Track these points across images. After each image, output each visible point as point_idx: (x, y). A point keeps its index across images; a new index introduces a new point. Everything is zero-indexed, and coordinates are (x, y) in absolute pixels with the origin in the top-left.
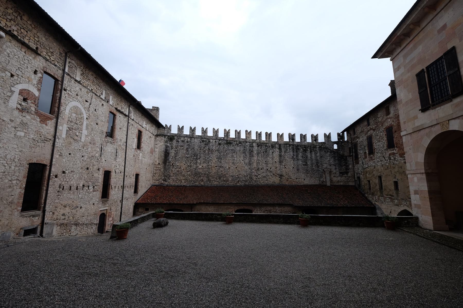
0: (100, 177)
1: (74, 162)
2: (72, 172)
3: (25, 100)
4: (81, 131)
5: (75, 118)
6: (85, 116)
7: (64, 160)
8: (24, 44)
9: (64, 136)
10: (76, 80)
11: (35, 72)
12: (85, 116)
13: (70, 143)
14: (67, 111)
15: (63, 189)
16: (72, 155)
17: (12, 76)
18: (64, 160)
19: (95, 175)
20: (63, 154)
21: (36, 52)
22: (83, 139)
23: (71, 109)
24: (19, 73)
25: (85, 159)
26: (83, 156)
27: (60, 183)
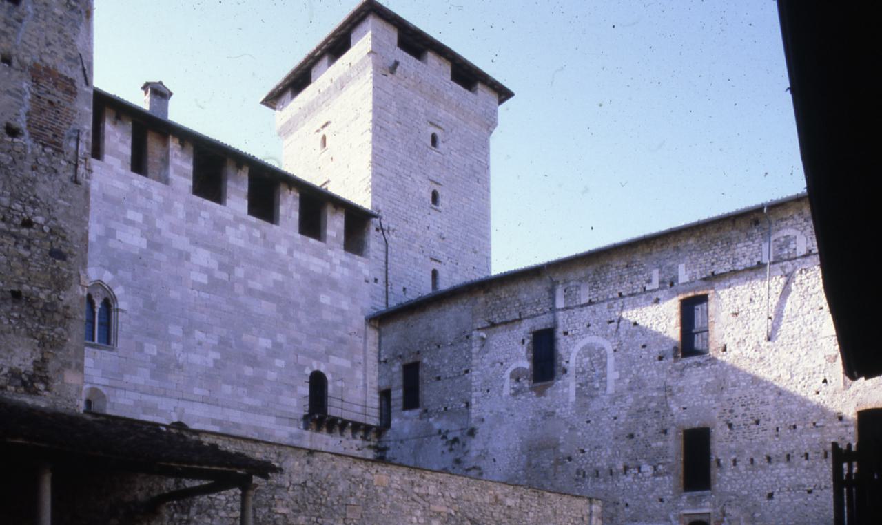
0: (673, 447)
1: (598, 431)
2: (596, 448)
3: (518, 380)
4: (604, 379)
5: (589, 363)
6: (609, 350)
7: (579, 434)
8: (506, 323)
9: (573, 398)
10: (582, 306)
11: (523, 342)
12: (609, 350)
13: (586, 405)
14: (572, 361)
15: (584, 476)
16: (593, 422)
17: (502, 364)
18: (579, 434)
19: (654, 445)
20: (576, 426)
21: (520, 320)
22: (611, 389)
23: (579, 354)
24: (508, 356)
25: (622, 421)
26: (615, 418)
27: (578, 467)
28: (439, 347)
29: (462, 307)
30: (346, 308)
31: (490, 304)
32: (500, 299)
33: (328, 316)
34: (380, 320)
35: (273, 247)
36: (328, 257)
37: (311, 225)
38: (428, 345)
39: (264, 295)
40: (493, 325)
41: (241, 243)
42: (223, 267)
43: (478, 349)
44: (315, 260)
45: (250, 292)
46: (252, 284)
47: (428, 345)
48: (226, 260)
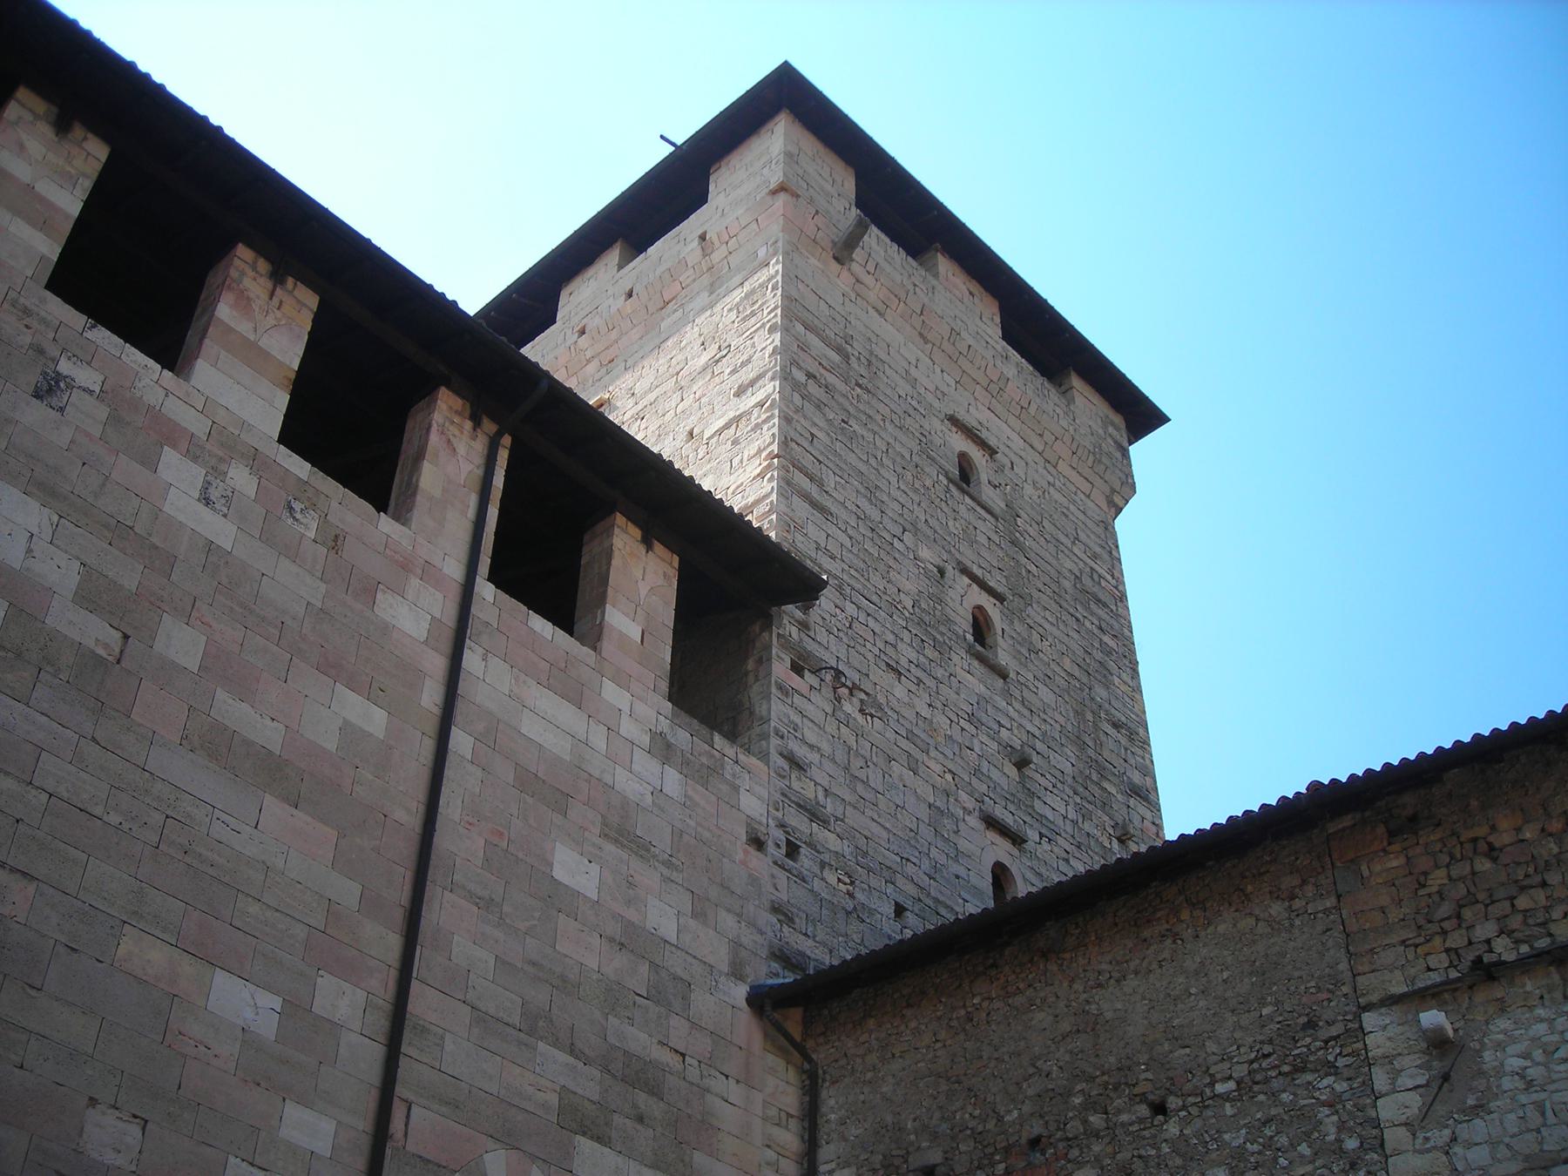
28: (1160, 1109)
29: (1277, 909)
30: (669, 930)
31: (1438, 878)
32: (1492, 852)
33: (586, 953)
34: (811, 1005)
35: (369, 592)
36: (587, 702)
37: (539, 559)
38: (1090, 1105)
39: (275, 773)
40: (1487, 972)
41: (221, 530)
42: (91, 596)
43: (1415, 1101)
44: (547, 702)
45: (219, 746)
46: (231, 710)
47: (1090, 1105)
48: (129, 576)
